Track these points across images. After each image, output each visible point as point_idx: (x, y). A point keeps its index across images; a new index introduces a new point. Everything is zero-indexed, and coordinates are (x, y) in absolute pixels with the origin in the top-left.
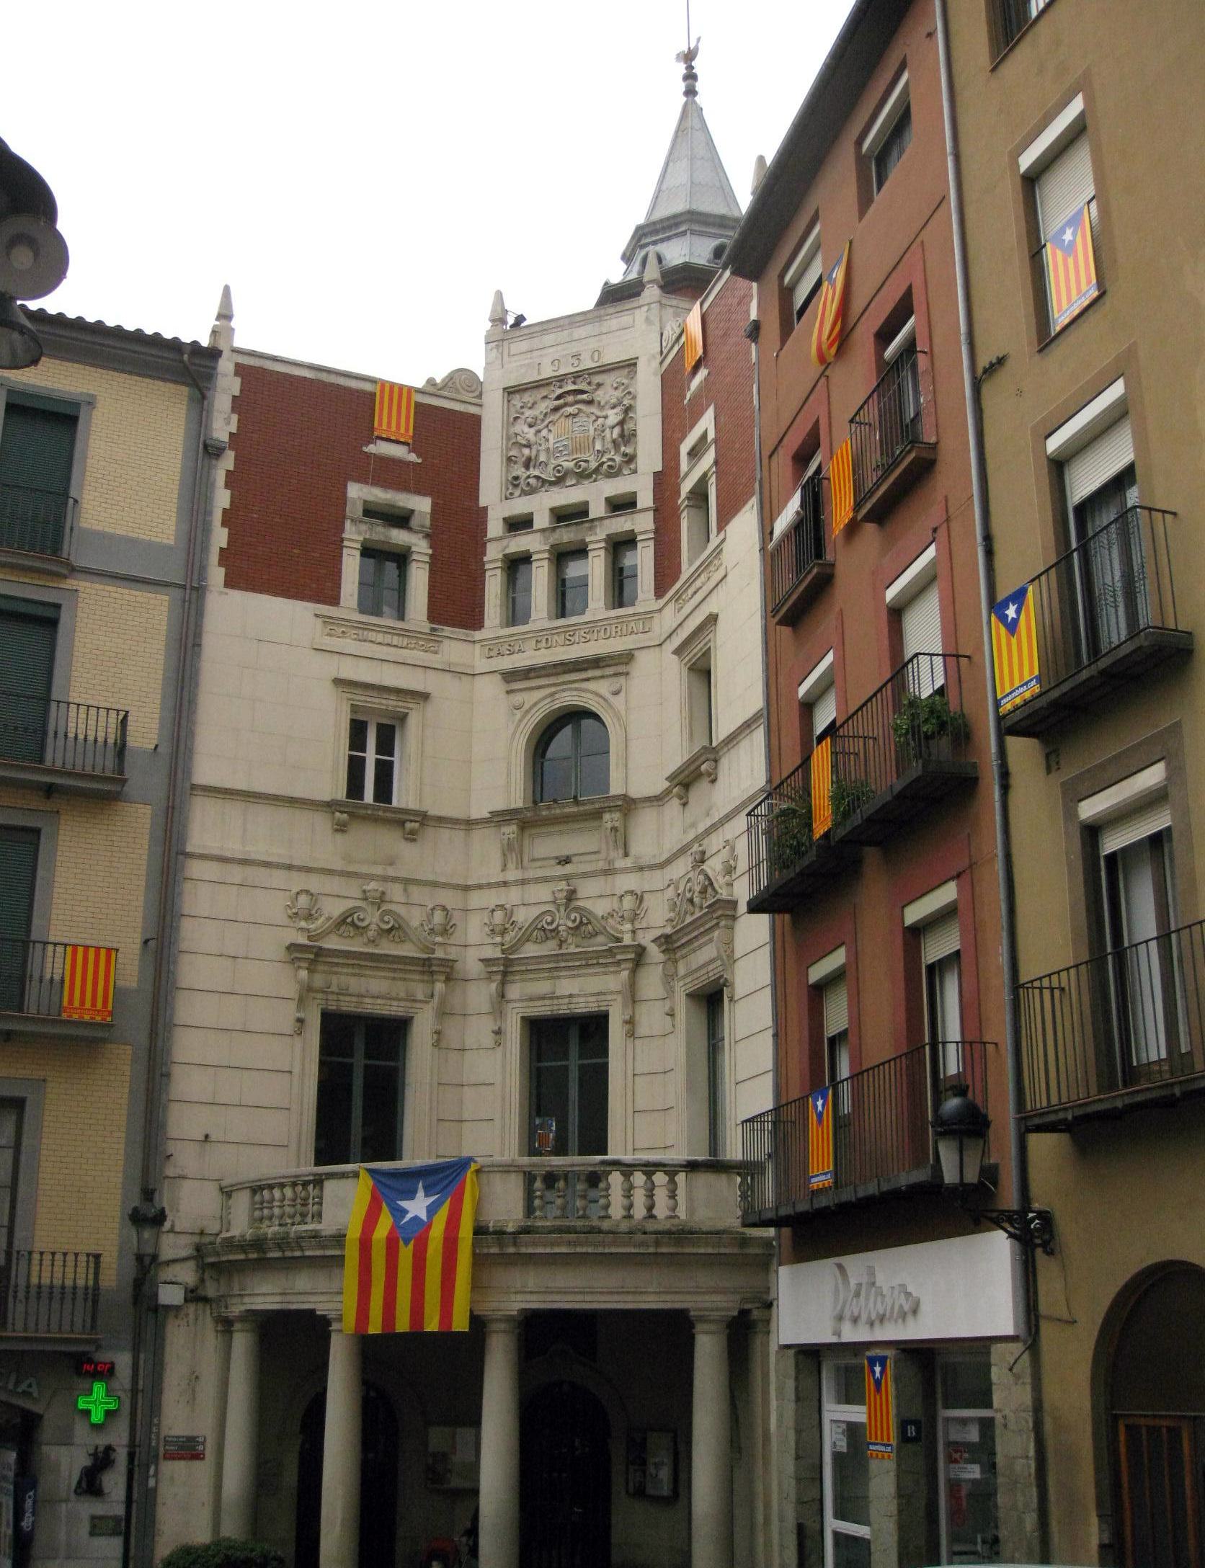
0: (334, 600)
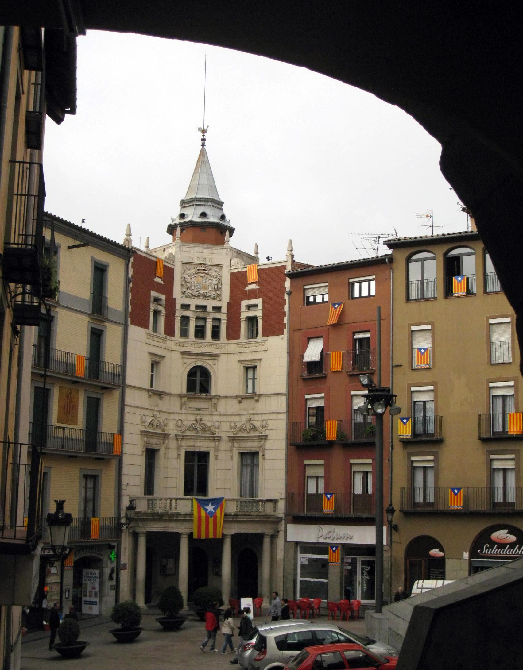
0: (147, 328)
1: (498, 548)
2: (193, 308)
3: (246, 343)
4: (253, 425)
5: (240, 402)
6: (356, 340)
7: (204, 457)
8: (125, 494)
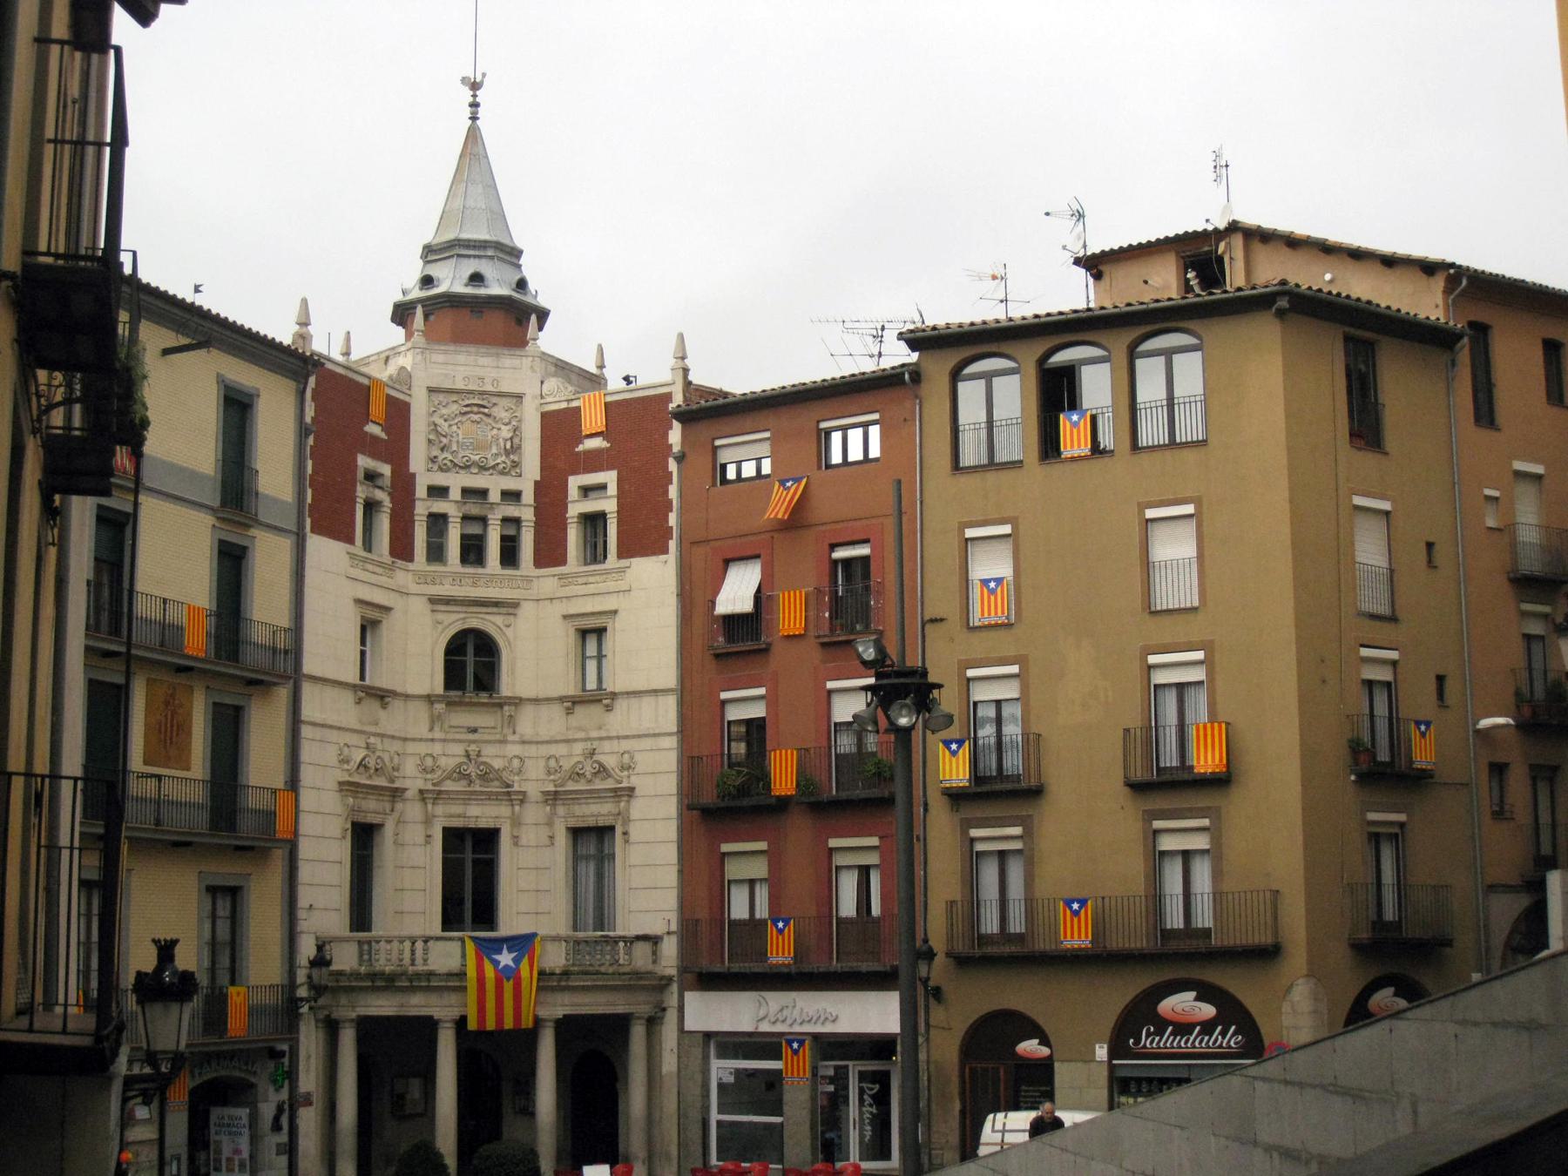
1: (1174, 1034)
2: (455, 494)
3: (577, 575)
4: (601, 765)
5: (569, 712)
6: (836, 562)
7: (487, 839)
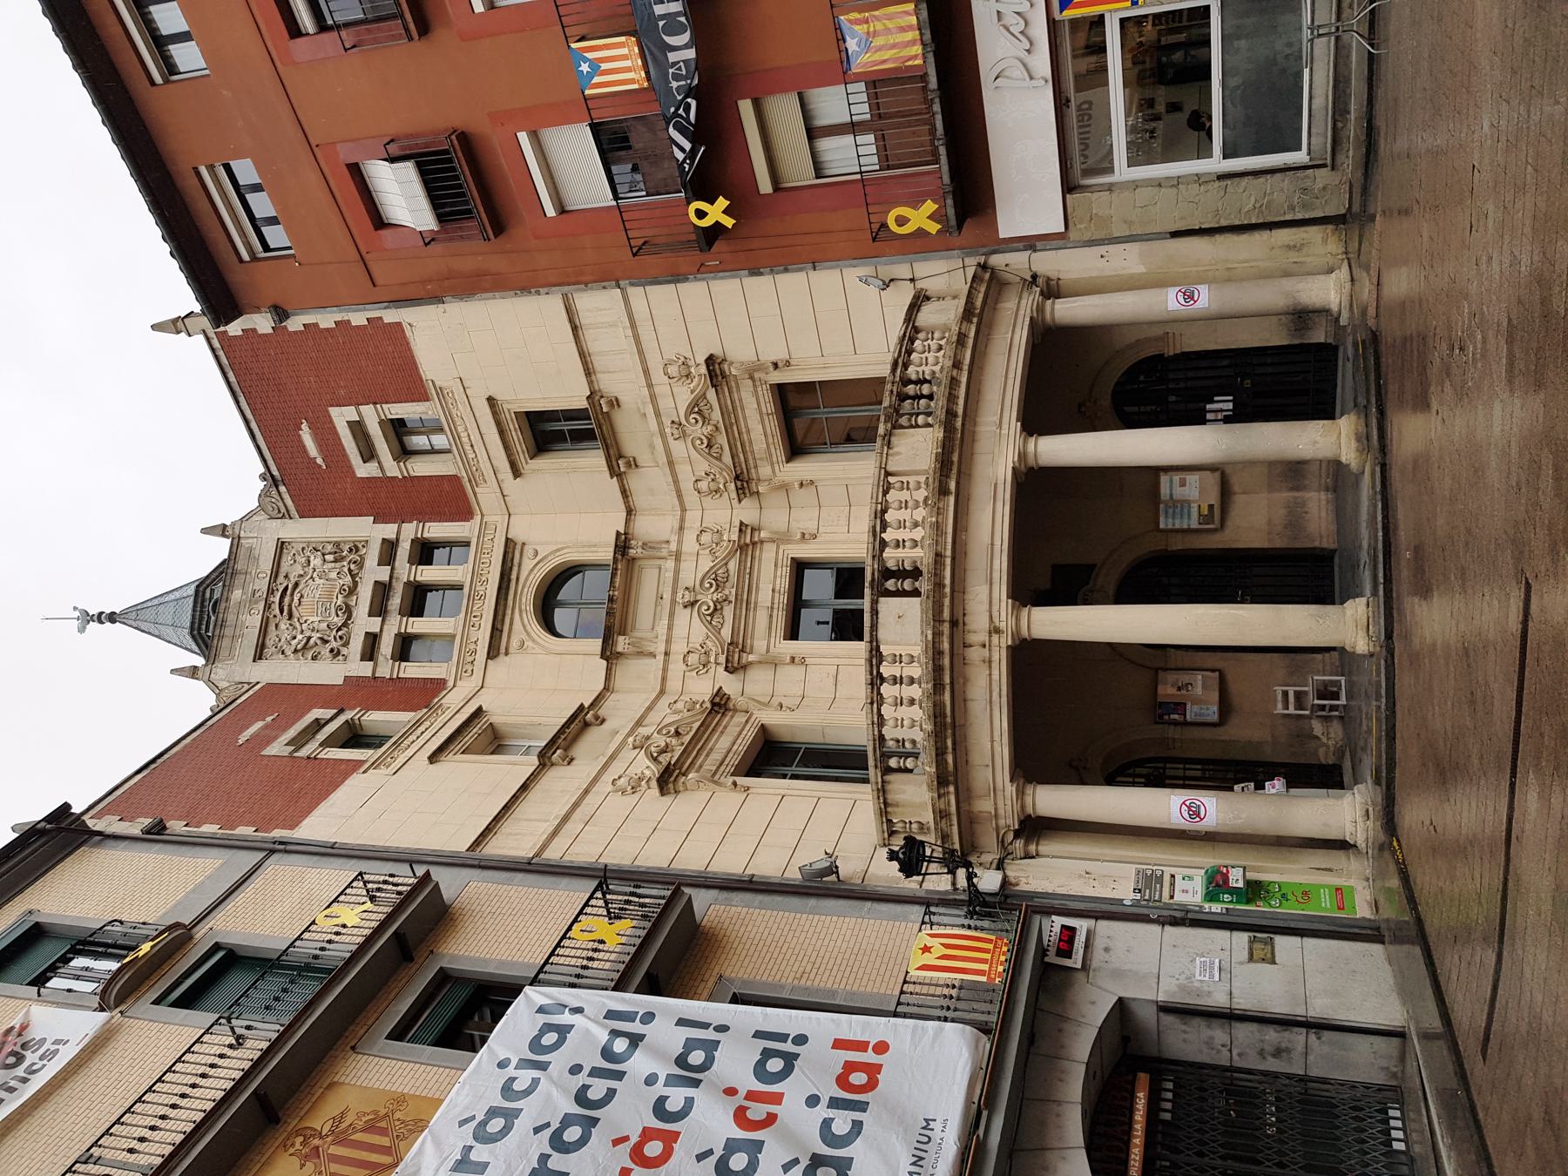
4: (689, 411)
5: (633, 464)
8: (861, 867)
